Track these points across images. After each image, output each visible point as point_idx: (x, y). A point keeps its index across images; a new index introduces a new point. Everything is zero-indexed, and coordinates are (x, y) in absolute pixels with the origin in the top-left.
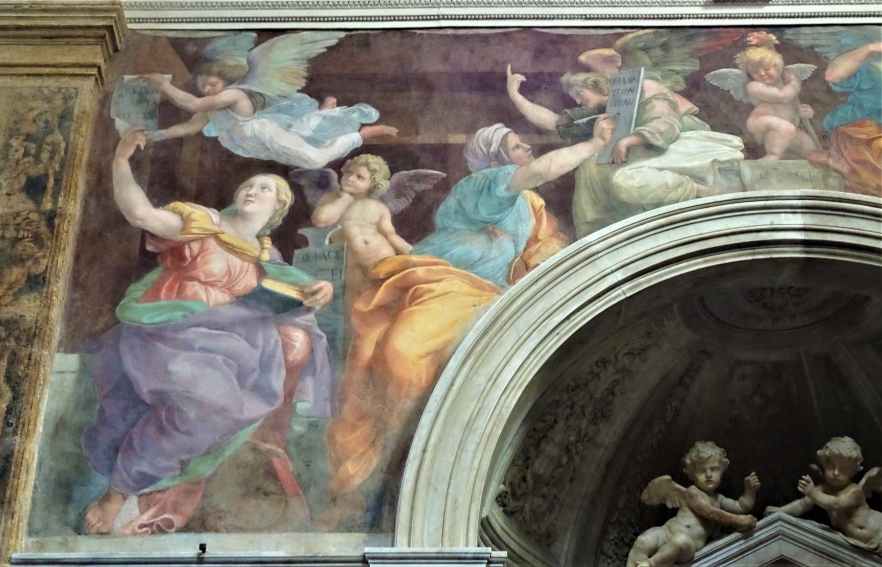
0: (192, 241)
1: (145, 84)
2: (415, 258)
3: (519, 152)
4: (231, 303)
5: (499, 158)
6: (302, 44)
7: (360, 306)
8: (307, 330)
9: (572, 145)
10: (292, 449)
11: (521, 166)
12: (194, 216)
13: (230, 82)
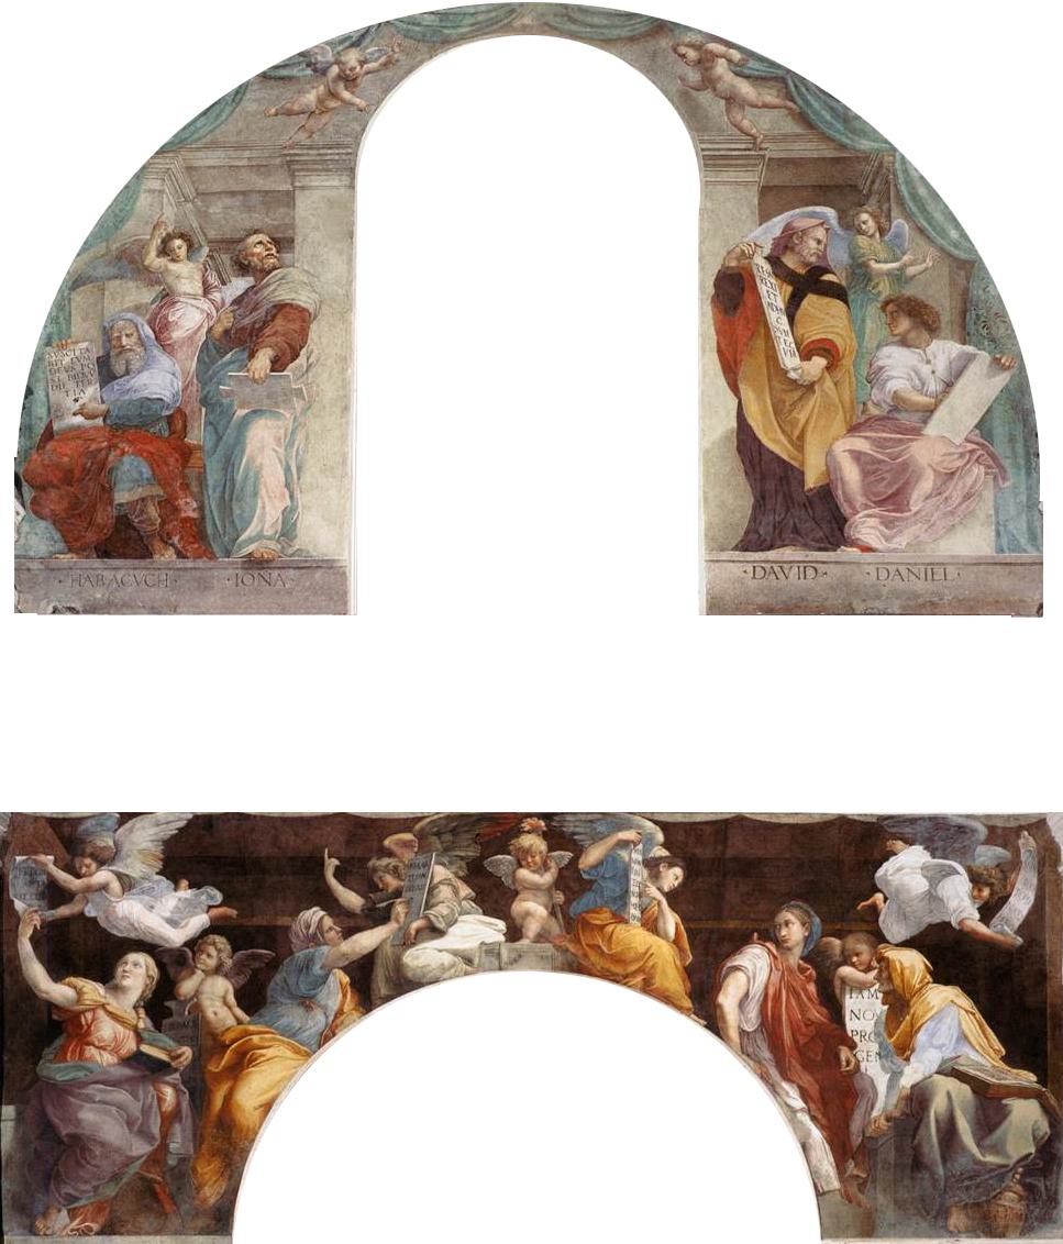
0: (86, 1011)
1: (33, 865)
2: (252, 1028)
3: (332, 933)
4: (119, 1064)
5: (316, 939)
6: (158, 825)
7: (213, 1068)
8: (174, 1086)
9: (372, 928)
10: (167, 1177)
11: (333, 946)
12: (85, 990)
13: (102, 863)
